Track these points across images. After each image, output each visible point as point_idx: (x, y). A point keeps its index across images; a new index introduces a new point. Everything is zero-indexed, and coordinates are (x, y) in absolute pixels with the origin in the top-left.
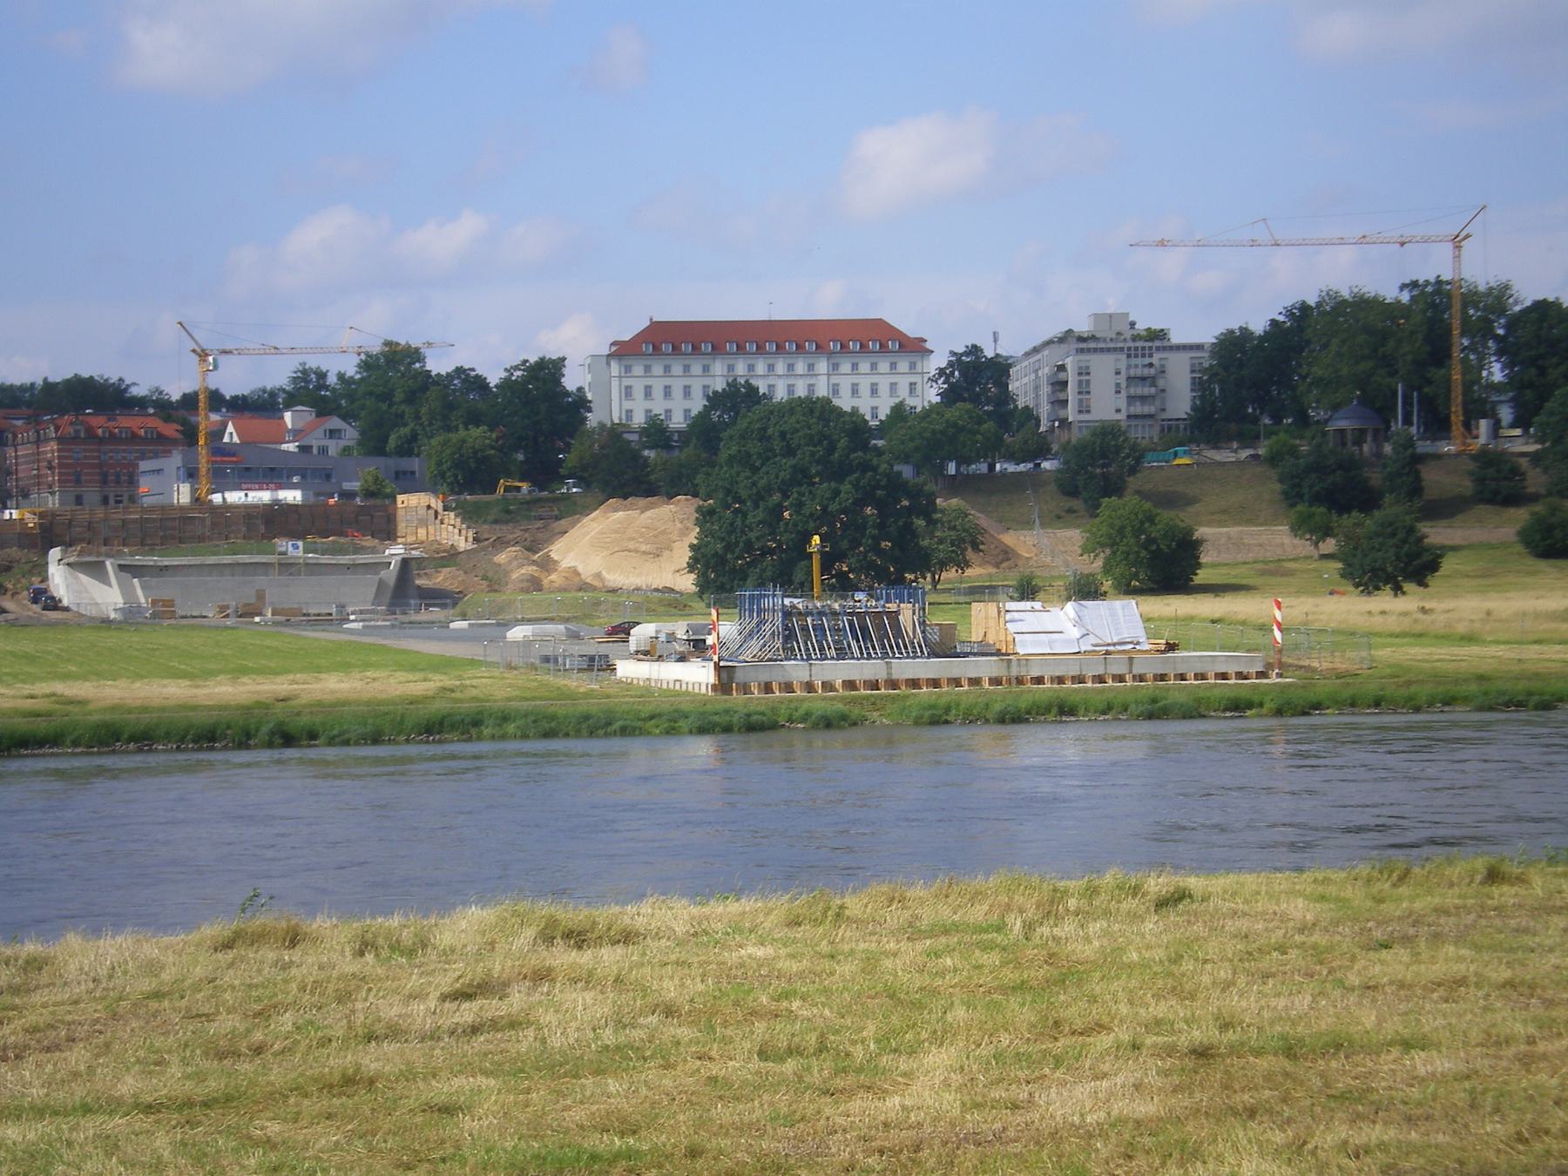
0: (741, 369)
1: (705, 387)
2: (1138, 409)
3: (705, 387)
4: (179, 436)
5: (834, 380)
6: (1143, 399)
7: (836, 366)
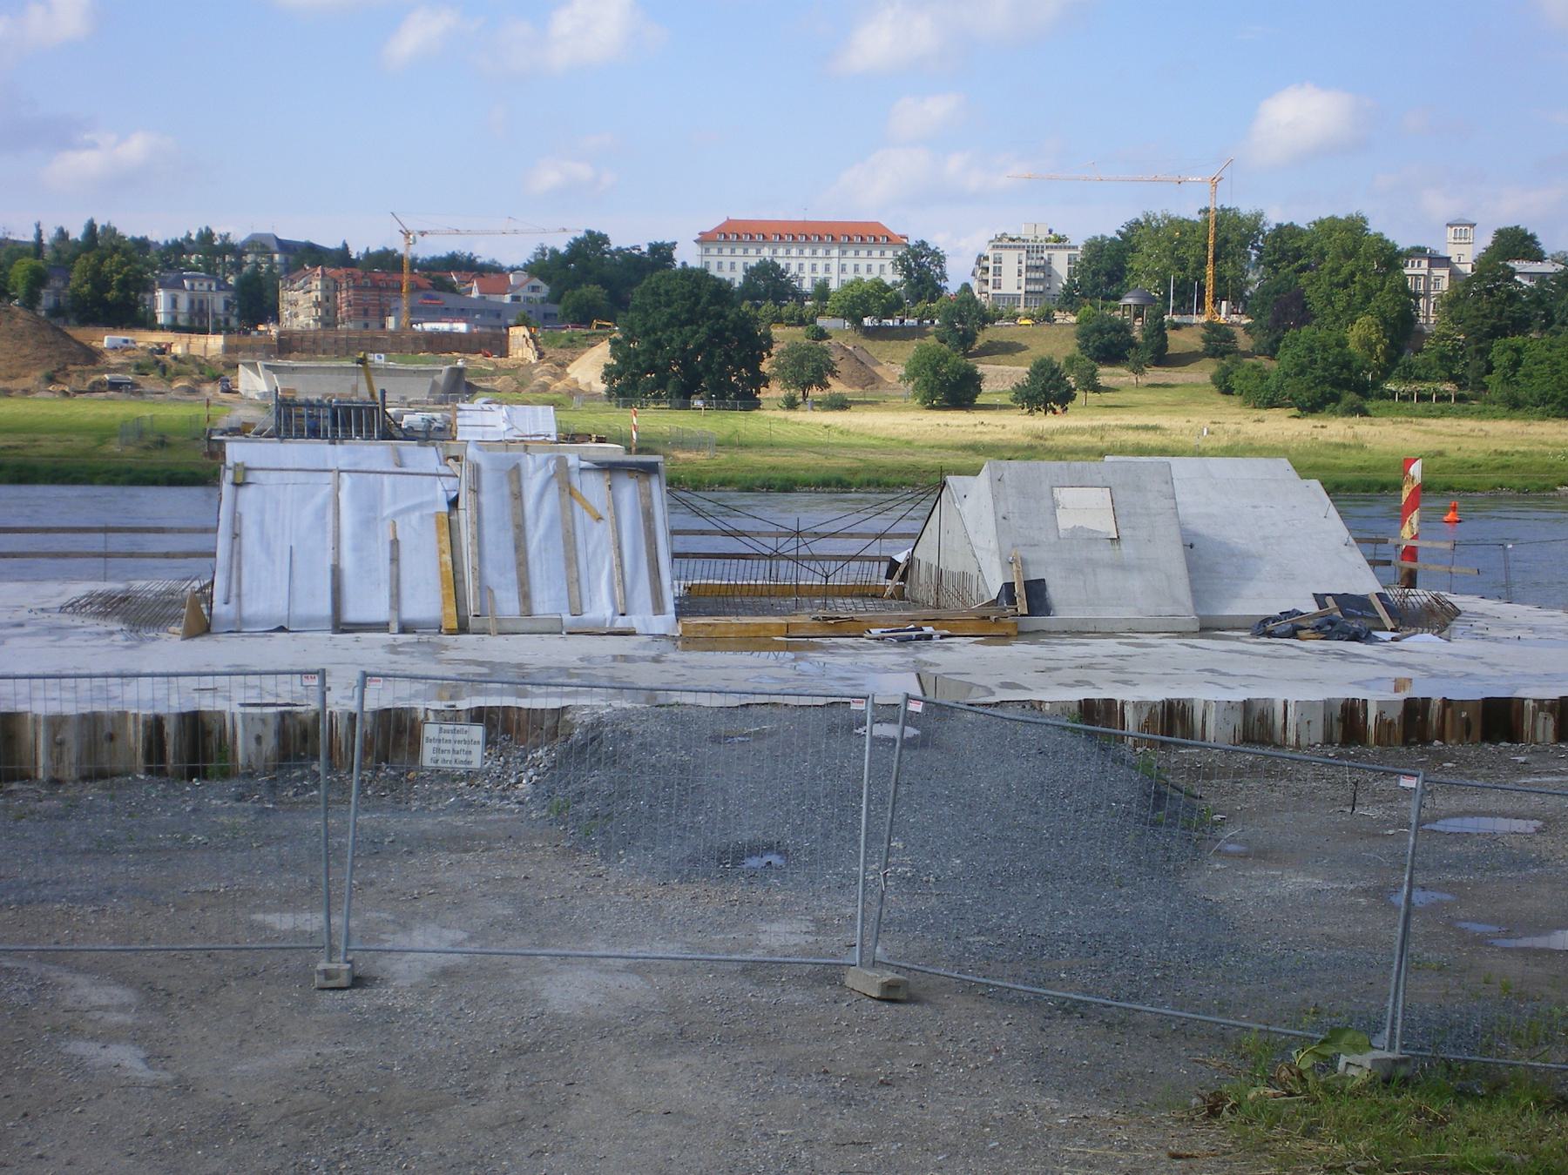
0: (781, 252)
1: (745, 264)
2: (1031, 288)
3: (745, 264)
4: (429, 286)
5: (843, 261)
6: (1037, 281)
7: (844, 252)
